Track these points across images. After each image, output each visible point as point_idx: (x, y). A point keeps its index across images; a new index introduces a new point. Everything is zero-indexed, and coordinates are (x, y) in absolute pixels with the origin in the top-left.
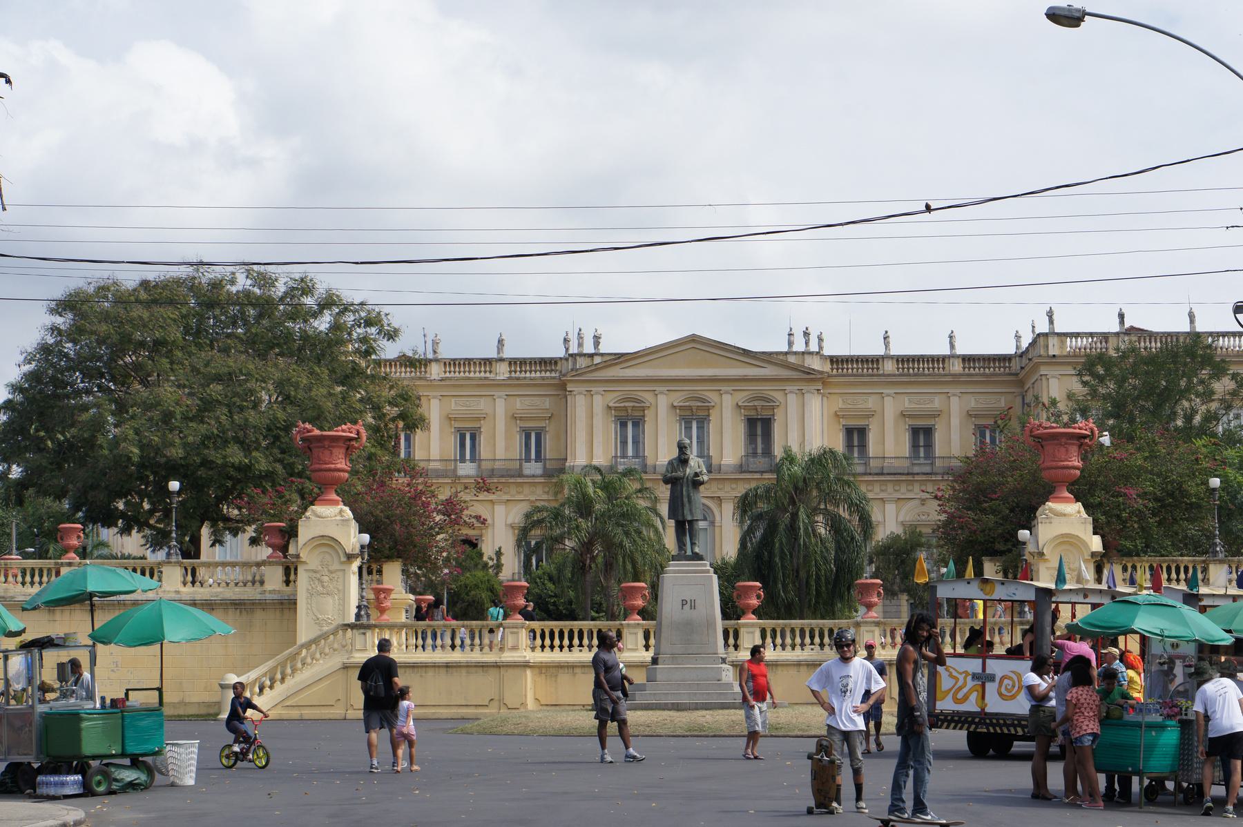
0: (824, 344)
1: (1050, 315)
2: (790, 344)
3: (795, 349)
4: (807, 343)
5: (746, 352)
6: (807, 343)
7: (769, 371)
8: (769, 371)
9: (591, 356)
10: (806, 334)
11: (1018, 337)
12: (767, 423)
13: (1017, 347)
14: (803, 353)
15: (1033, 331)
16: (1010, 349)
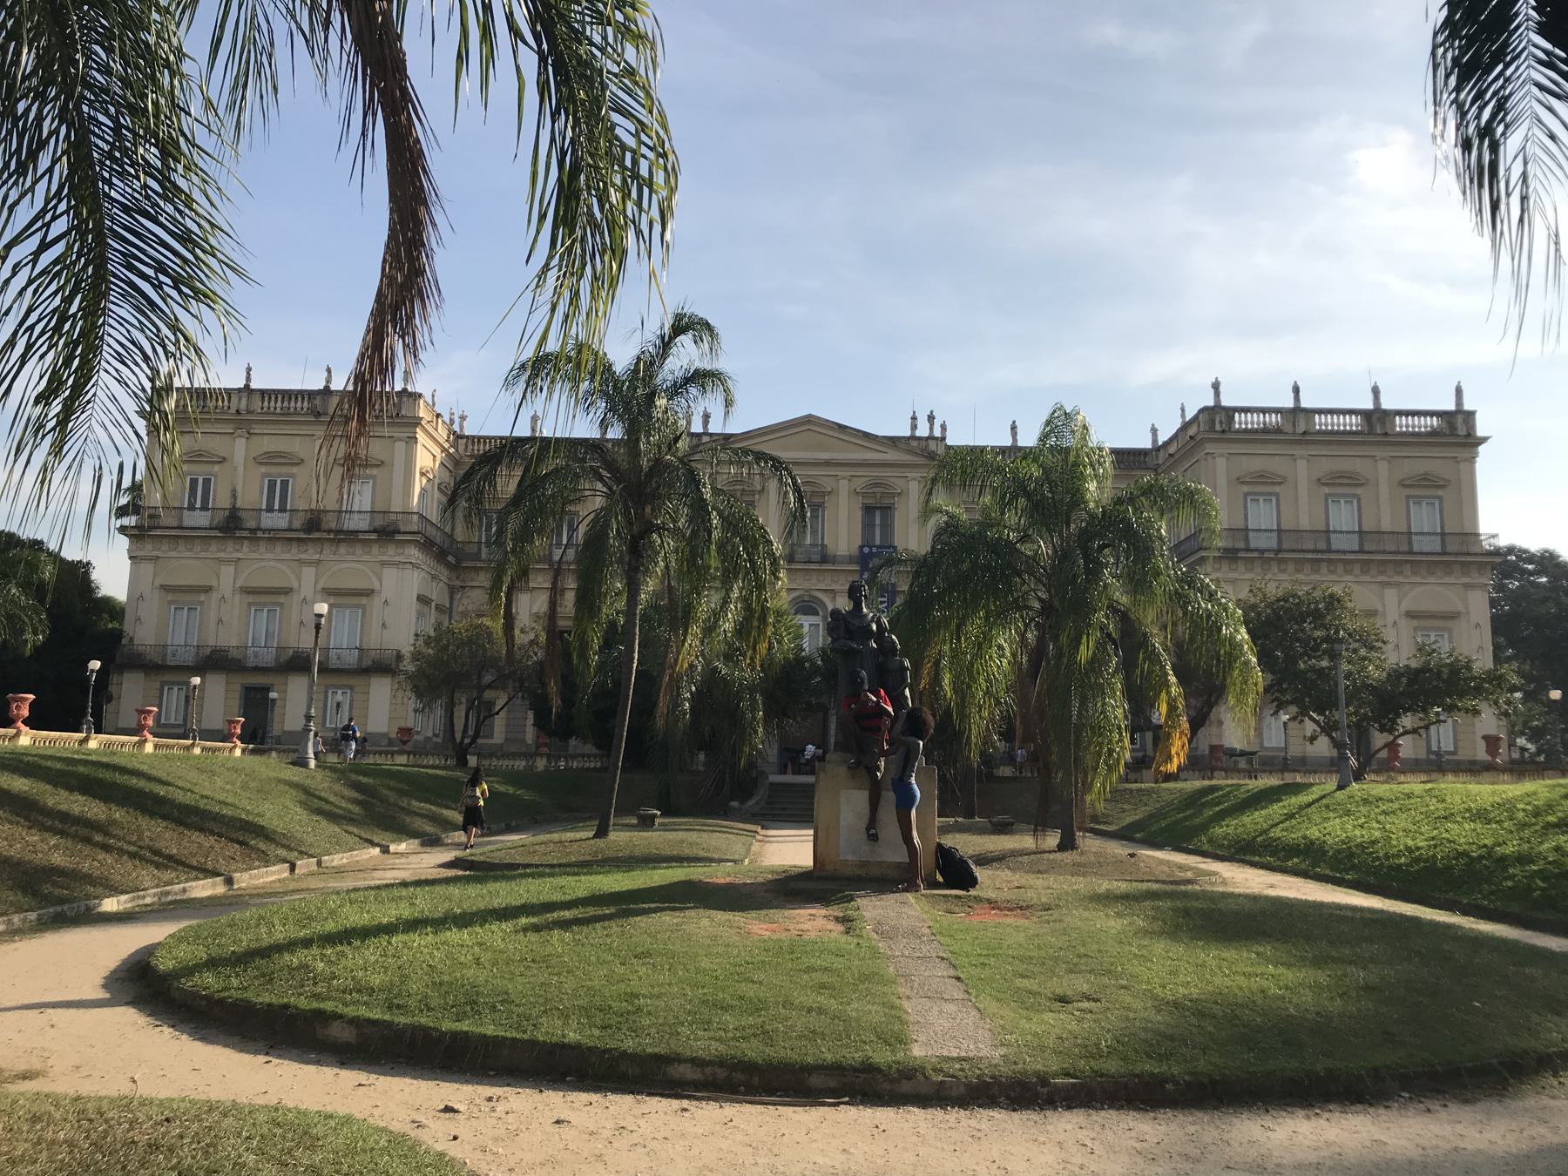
0: (948, 434)
1: (1216, 386)
2: (914, 427)
3: (918, 433)
4: (931, 429)
5: (866, 435)
6: (931, 429)
7: (891, 455)
8: (891, 455)
9: (698, 435)
10: (931, 418)
11: (1154, 431)
12: (887, 510)
13: (1155, 440)
14: (927, 439)
15: (1183, 415)
16: (1149, 445)
